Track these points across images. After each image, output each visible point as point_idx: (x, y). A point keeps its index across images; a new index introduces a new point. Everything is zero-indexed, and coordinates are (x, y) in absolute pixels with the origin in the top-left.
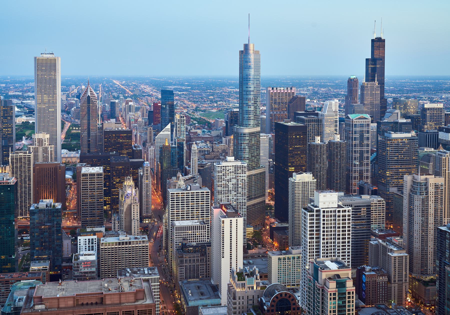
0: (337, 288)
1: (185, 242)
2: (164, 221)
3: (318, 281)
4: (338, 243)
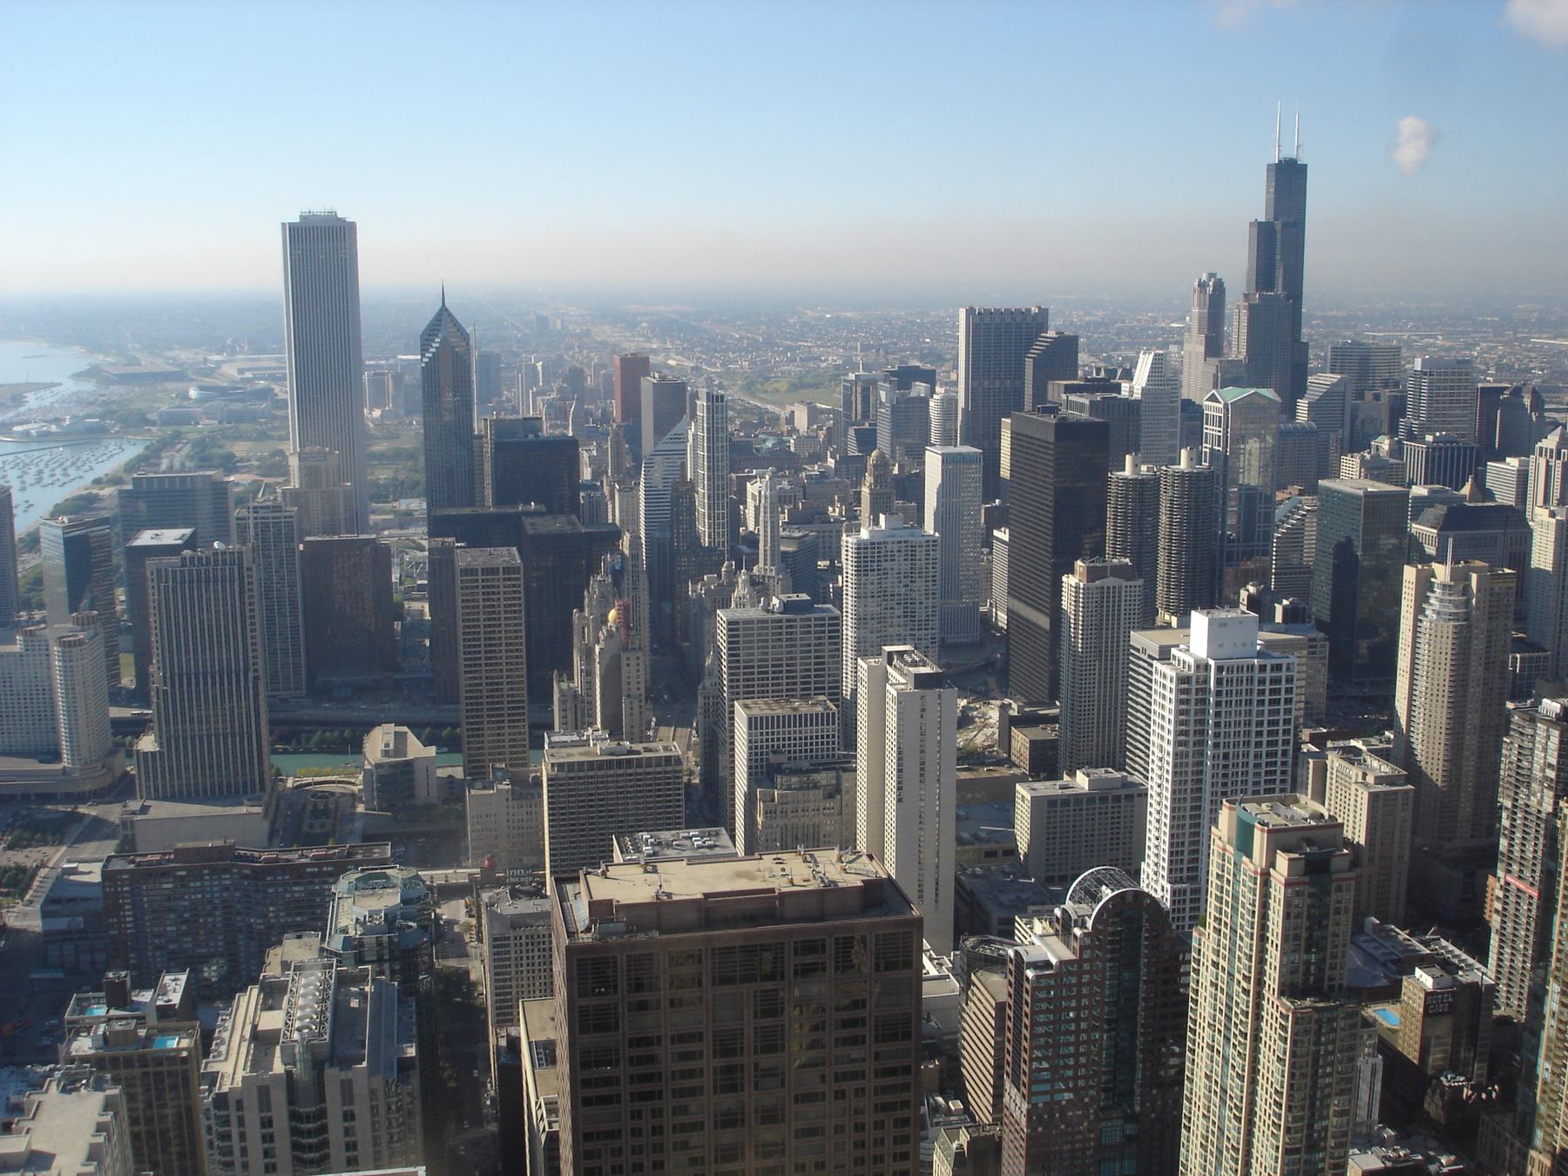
0: (1306, 874)
1: (773, 759)
2: (701, 701)
3: (1250, 856)
4: (1256, 756)
